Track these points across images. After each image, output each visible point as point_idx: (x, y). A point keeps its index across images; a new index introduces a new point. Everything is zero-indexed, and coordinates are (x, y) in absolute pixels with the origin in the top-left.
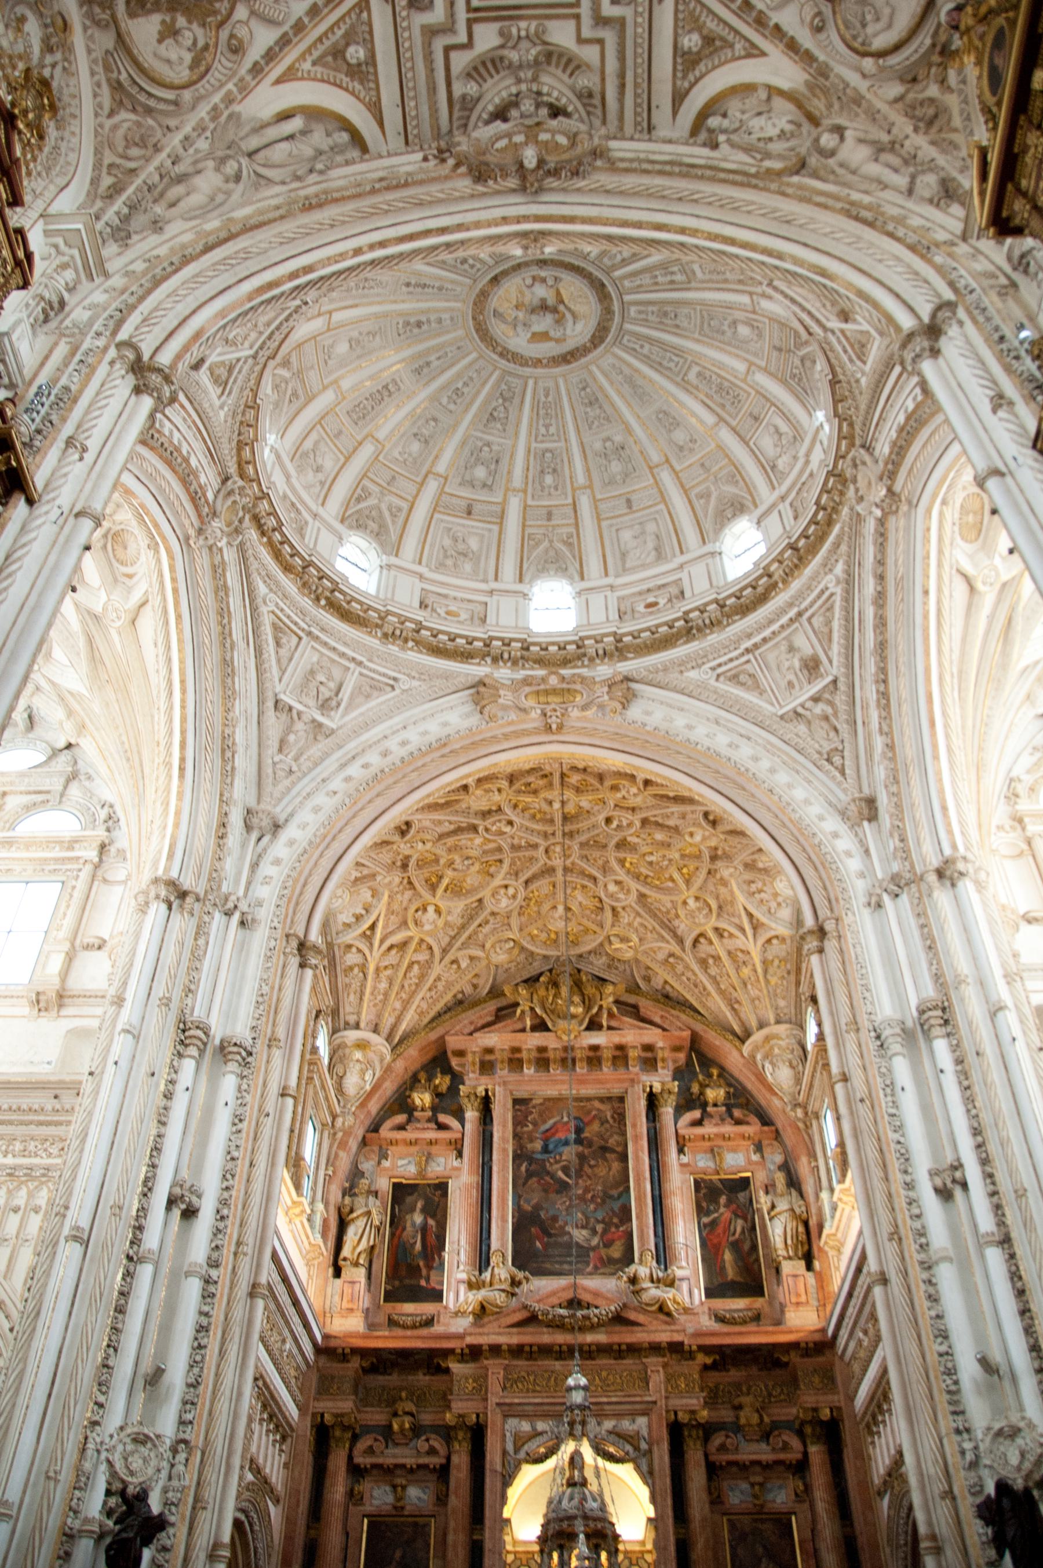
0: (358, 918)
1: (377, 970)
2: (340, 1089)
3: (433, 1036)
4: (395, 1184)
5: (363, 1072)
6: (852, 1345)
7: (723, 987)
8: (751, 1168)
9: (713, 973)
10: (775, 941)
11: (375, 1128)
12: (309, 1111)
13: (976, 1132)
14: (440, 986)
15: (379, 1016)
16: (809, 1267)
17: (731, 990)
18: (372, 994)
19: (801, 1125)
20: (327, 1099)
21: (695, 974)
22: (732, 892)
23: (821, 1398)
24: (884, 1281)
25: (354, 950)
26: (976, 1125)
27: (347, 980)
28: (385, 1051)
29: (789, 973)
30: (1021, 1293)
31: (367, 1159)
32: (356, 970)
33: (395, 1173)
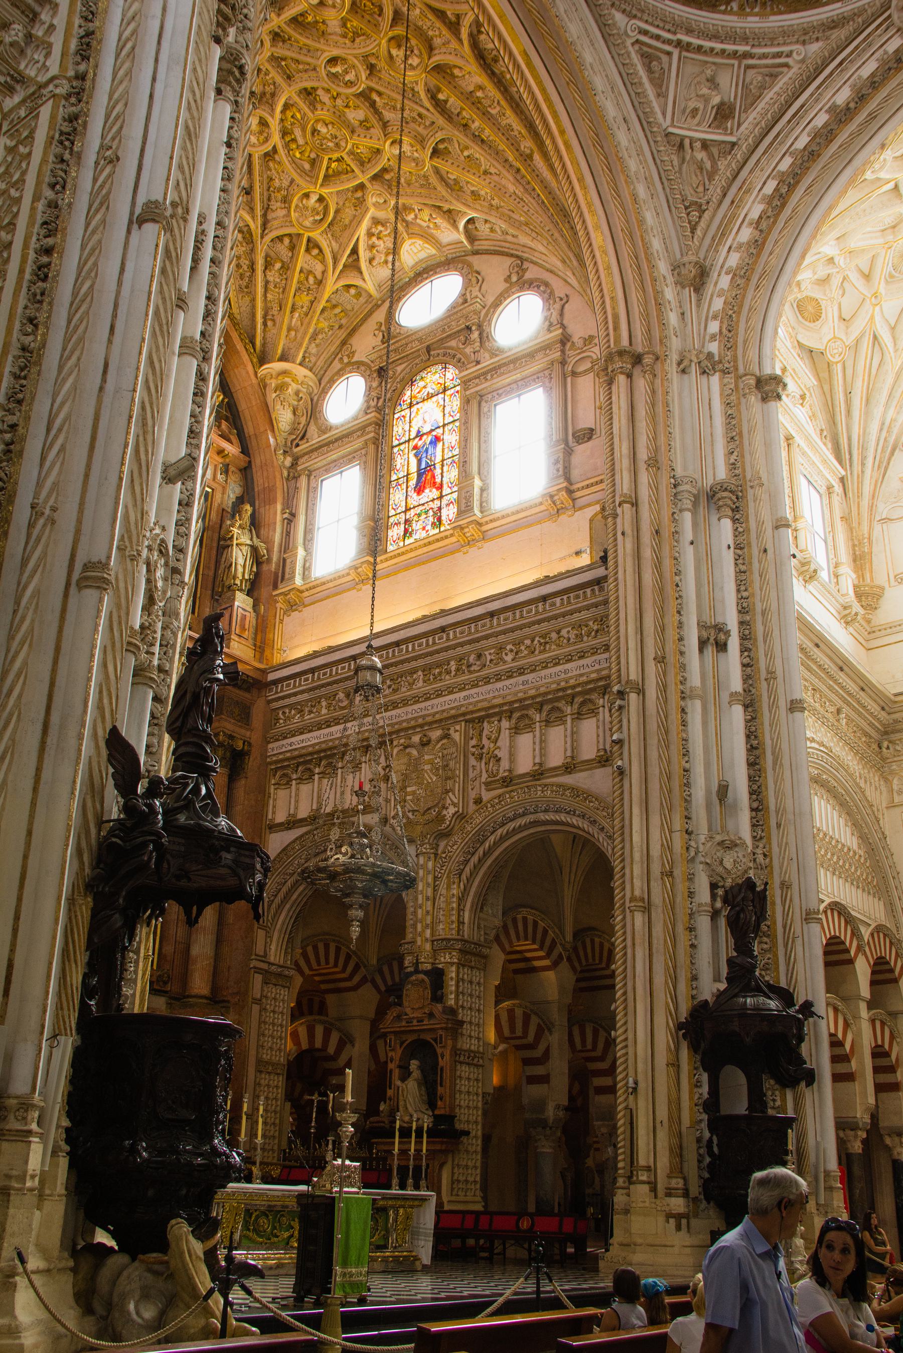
6: (300, 698)
7: (269, 297)
8: (214, 485)
9: (271, 279)
10: (353, 291)
13: (743, 611)
16: (255, 606)
17: (276, 308)
19: (285, 473)
21: (252, 267)
22: (356, 221)
23: (237, 729)
24: (641, 691)
26: (745, 605)
29: (340, 327)
30: (751, 749)
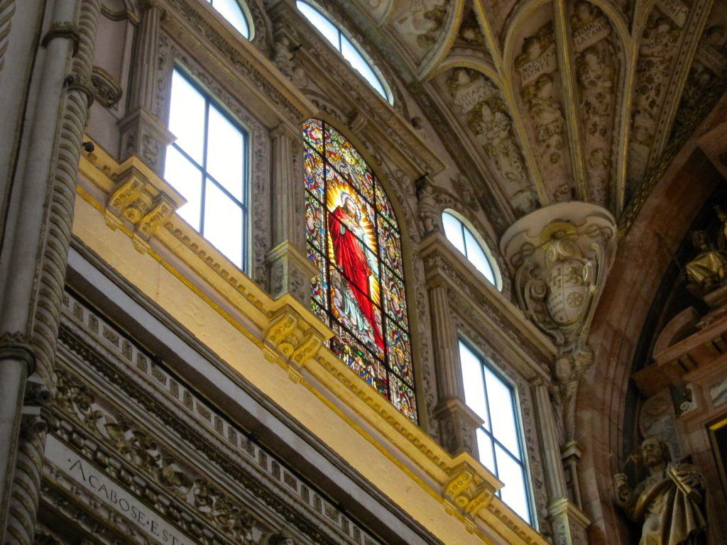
0: (439, 19)
1: (523, 92)
2: (548, 322)
3: (681, 160)
4: (718, 432)
5: (576, 273)
11: (643, 357)
12: (448, 325)
14: (657, 73)
15: (570, 176)
18: (538, 141)
20: (506, 324)
25: (463, 78)
27: (481, 139)
28: (603, 222)
31: (655, 417)
32: (486, 111)
33: (712, 413)
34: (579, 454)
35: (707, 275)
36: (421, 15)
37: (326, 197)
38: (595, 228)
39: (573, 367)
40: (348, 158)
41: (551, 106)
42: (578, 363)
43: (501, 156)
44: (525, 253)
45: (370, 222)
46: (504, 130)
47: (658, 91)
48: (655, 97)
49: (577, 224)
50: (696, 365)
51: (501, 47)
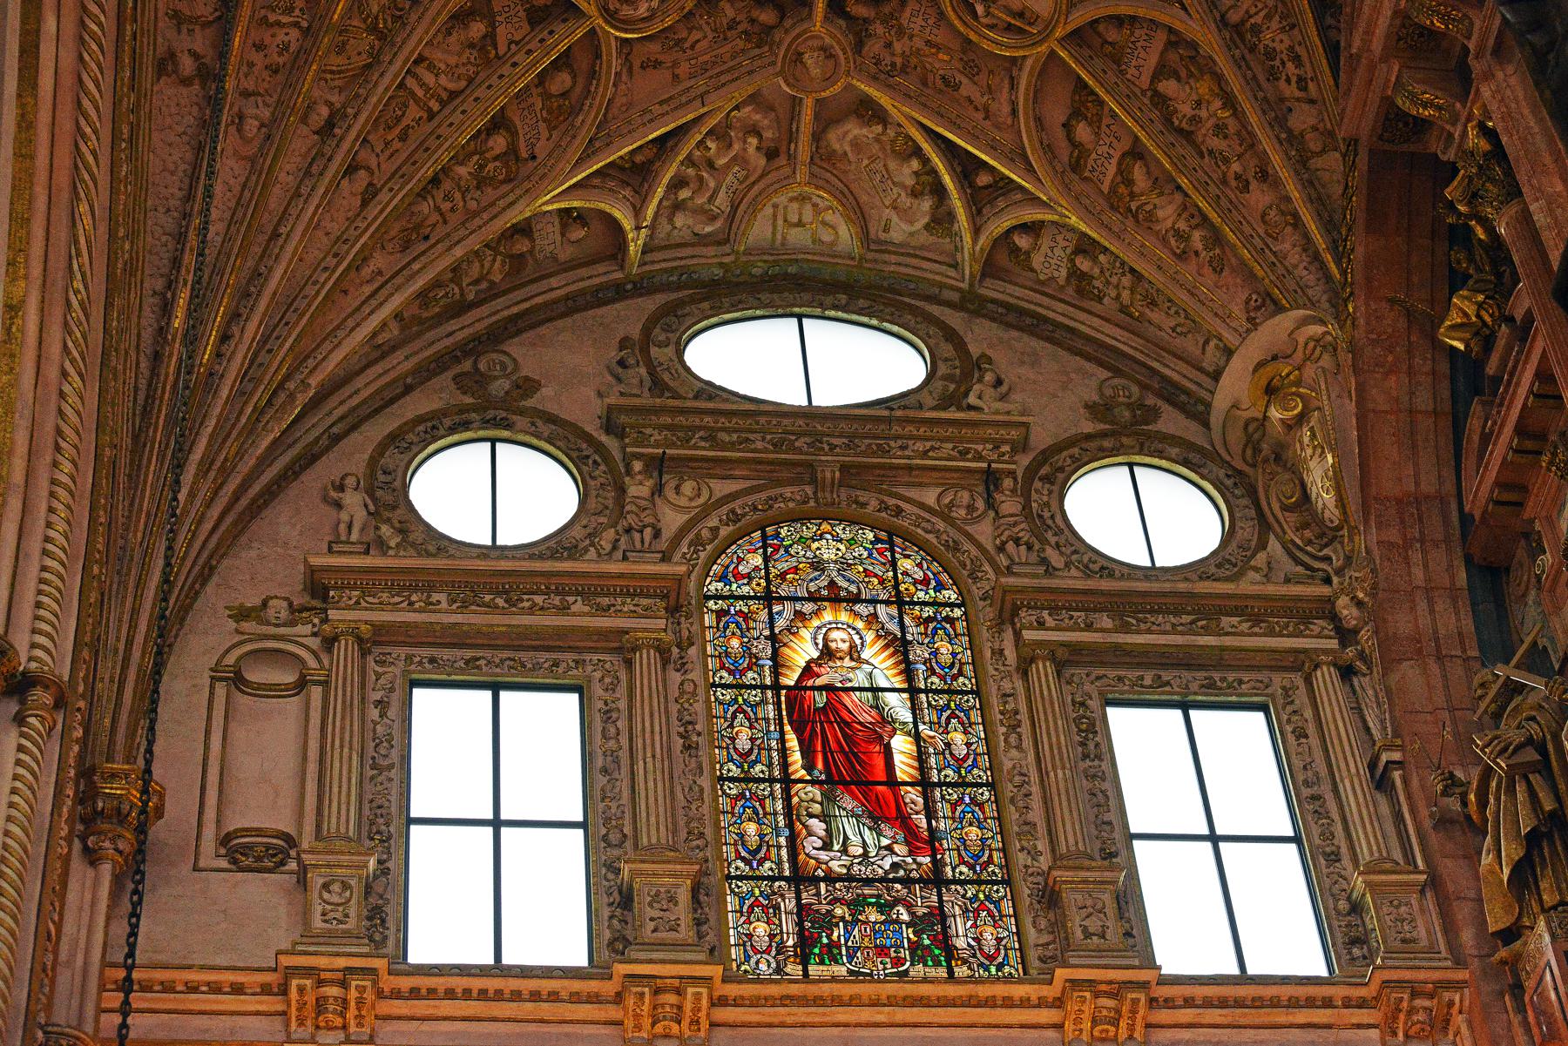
14: (1273, 37)
28: (1317, 330)
32: (1084, 264)
34: (1397, 756)
35: (1468, 335)
36: (906, 201)
37: (778, 665)
38: (1312, 344)
39: (1359, 604)
40: (828, 551)
41: (1161, 194)
42: (1361, 595)
43: (1147, 311)
44: (1256, 436)
45: (888, 633)
46: (1123, 274)
47: (1297, 60)
48: (1297, 72)
49: (1289, 352)
50: (1524, 489)
51: (1030, 169)
